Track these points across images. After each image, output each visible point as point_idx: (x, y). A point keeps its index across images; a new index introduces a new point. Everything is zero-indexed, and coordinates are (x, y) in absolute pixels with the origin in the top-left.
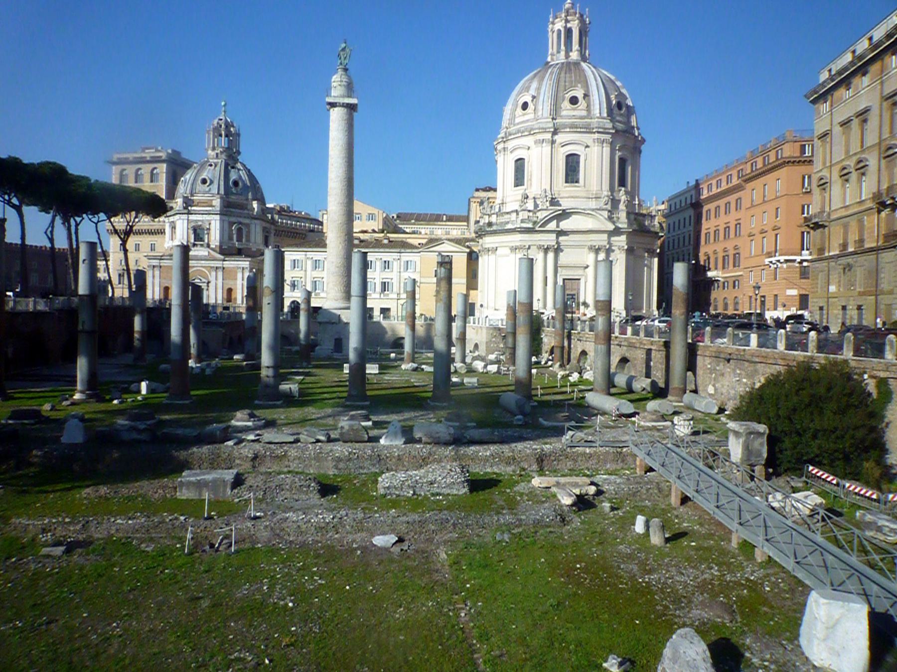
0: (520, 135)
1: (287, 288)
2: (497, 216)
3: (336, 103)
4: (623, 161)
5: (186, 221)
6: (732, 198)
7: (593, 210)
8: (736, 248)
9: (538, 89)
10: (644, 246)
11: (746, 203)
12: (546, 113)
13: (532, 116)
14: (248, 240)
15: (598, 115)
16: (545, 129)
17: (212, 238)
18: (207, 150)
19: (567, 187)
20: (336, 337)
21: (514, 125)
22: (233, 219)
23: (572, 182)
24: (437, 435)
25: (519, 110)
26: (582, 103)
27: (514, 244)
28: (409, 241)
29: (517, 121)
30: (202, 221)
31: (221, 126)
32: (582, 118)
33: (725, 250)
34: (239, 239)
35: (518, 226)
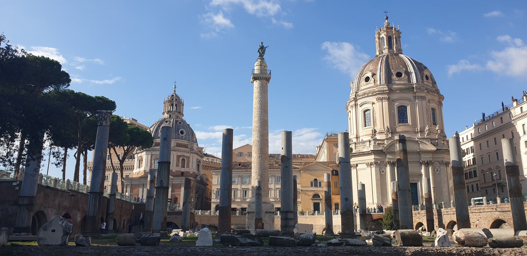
0: (366, 96)
2: (355, 145)
3: (258, 77)
4: (433, 110)
5: (150, 156)
12: (383, 81)
13: (373, 85)
14: (188, 167)
15: (416, 82)
16: (383, 91)
18: (164, 113)
19: (400, 126)
21: (361, 90)
22: (180, 154)
24: (476, 239)
25: (363, 82)
29: (362, 88)
31: (173, 99)
35: (372, 149)
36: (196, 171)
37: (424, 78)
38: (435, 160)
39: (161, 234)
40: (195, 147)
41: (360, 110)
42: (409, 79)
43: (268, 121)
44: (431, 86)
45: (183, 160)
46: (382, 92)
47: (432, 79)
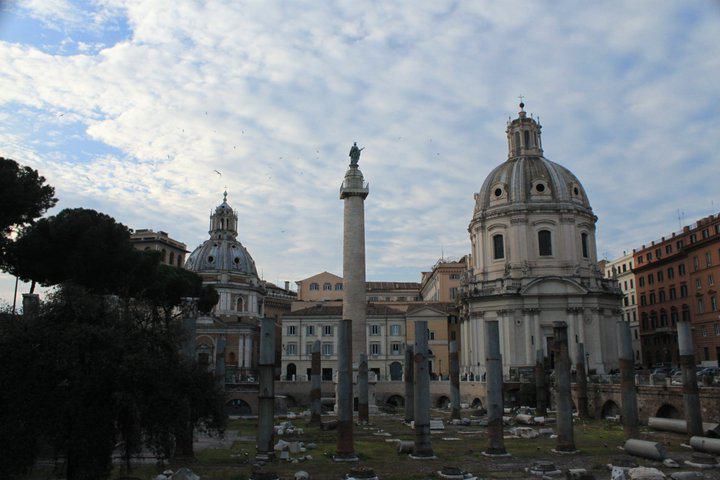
1: (284, 353)
4: (584, 236)
6: (675, 266)
7: (568, 277)
9: (509, 178)
13: (505, 201)
14: (246, 309)
25: (493, 196)
26: (547, 190)
28: (392, 307)
29: (492, 204)
34: (240, 309)
36: (257, 316)
37: (573, 192)
38: (587, 305)
39: (269, 456)
40: (255, 281)
41: (489, 235)
42: (553, 194)
44: (581, 203)
45: (240, 300)
46: (519, 212)
47: (583, 193)
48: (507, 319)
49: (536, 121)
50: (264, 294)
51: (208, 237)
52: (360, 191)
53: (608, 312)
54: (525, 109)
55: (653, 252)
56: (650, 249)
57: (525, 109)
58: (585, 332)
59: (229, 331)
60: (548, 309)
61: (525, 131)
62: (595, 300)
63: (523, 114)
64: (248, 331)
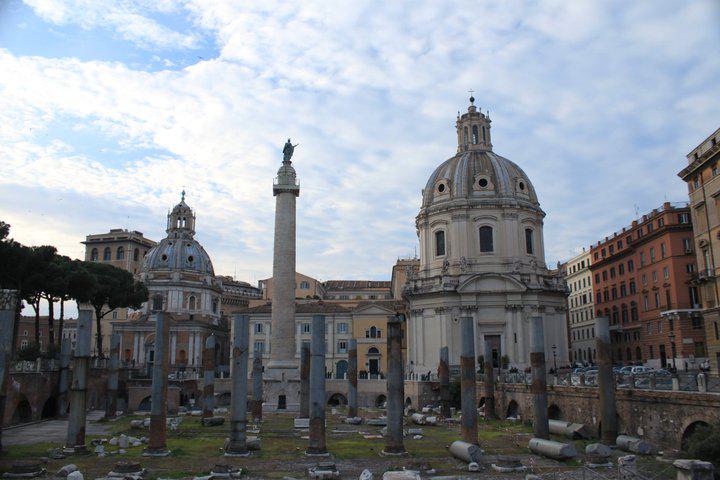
4: (529, 232)
6: (625, 262)
7: (507, 274)
8: (633, 303)
9: (453, 174)
10: (554, 305)
11: (637, 264)
13: (448, 196)
14: (199, 307)
17: (169, 306)
20: (281, 393)
23: (488, 250)
25: (436, 192)
26: (490, 185)
27: (438, 306)
29: (435, 200)
30: (161, 292)
32: (489, 197)
33: (623, 306)
34: (192, 307)
40: (209, 279)
43: (295, 252)
45: (192, 298)
48: (444, 316)
49: (486, 115)
50: (220, 292)
51: (166, 236)
52: (290, 188)
53: (552, 310)
54: (475, 104)
55: (607, 248)
56: (612, 240)
57: (475, 104)
58: (523, 329)
59: (180, 329)
60: (485, 307)
61: (474, 125)
62: (535, 298)
63: (472, 109)
64: (197, 329)
